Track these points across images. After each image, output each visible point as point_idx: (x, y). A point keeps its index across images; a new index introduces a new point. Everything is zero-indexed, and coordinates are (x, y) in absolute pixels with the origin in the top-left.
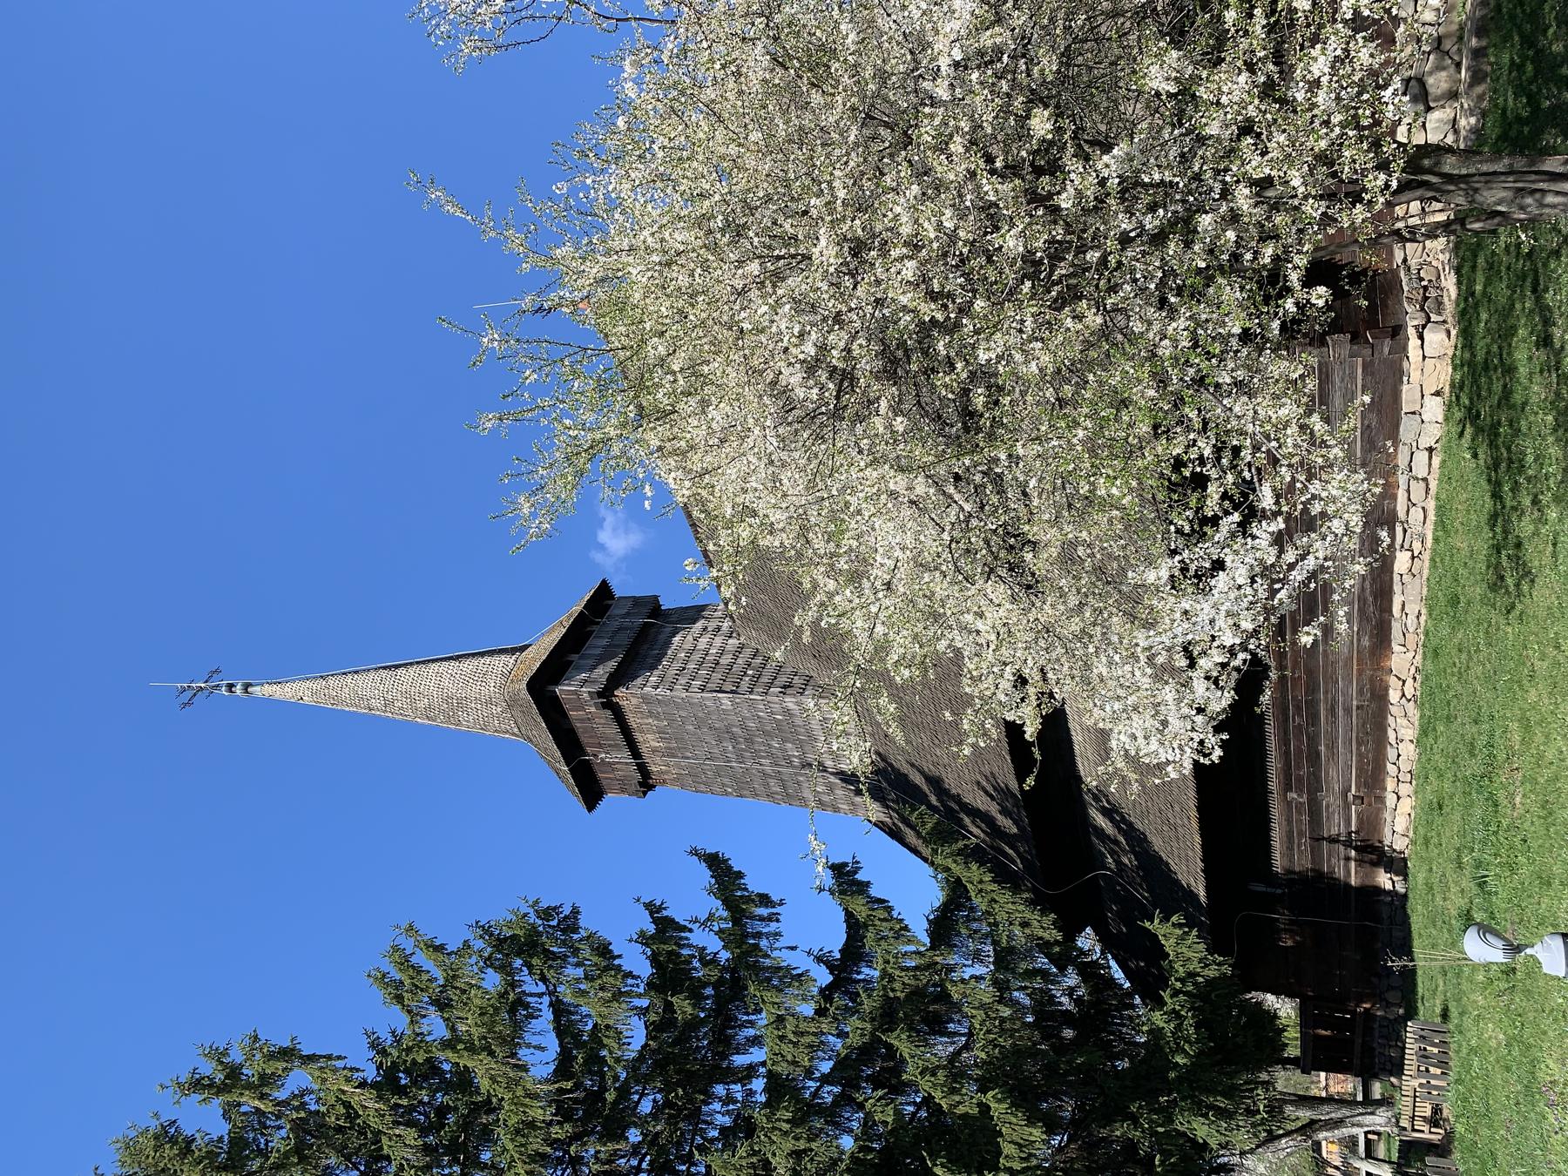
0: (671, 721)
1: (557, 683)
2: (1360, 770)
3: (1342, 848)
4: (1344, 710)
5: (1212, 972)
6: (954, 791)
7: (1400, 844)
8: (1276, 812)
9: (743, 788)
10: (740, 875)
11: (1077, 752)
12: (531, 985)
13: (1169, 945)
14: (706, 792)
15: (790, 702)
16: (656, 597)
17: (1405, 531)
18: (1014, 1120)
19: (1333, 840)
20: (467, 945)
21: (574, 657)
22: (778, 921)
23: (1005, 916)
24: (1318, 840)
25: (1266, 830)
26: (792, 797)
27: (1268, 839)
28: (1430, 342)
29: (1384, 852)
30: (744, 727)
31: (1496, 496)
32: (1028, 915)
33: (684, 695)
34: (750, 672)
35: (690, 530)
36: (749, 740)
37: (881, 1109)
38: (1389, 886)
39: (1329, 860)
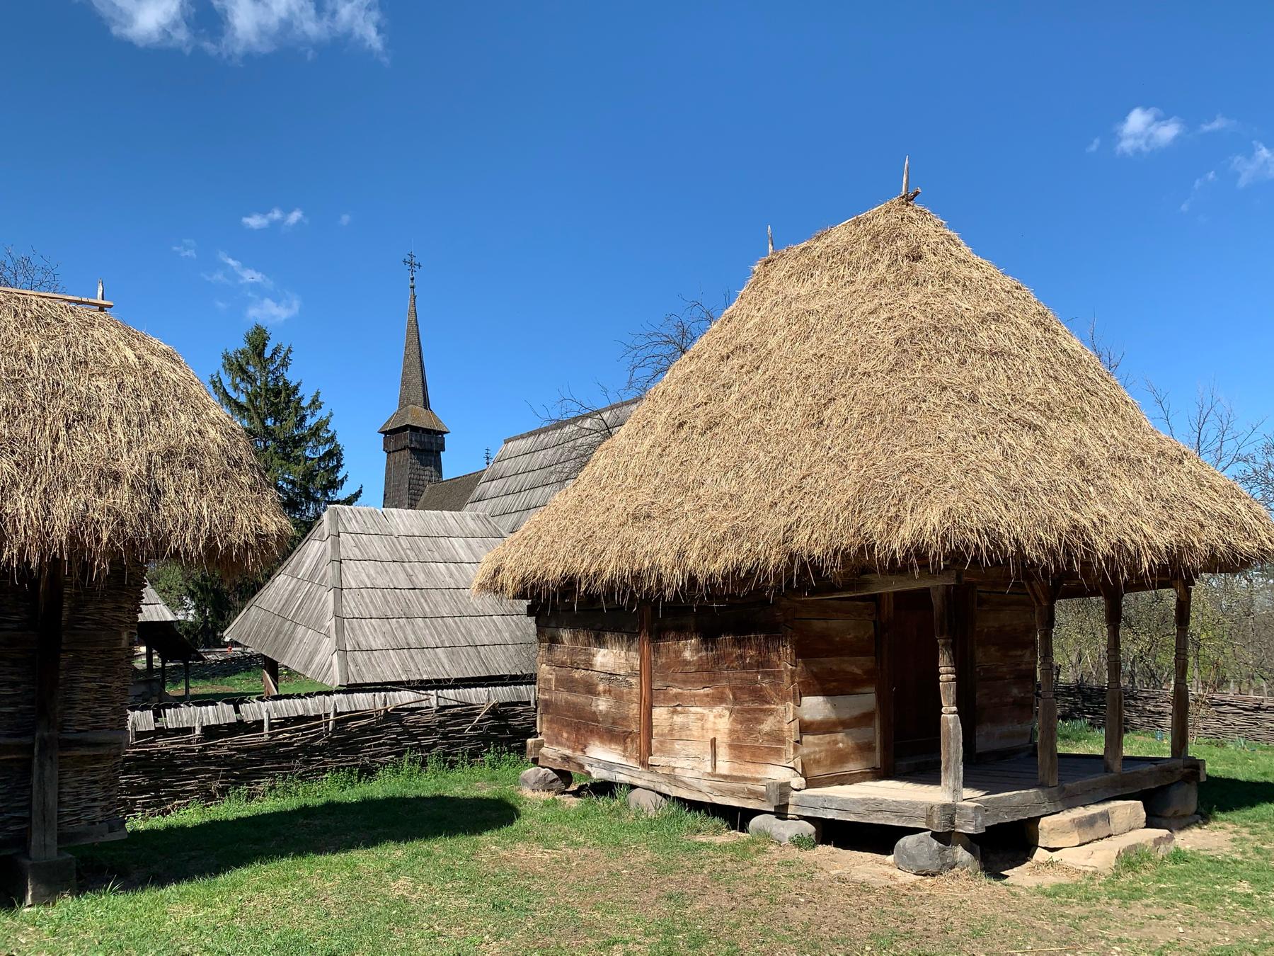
0: (402, 466)
9: (387, 484)
20: (329, 431)
21: (421, 431)
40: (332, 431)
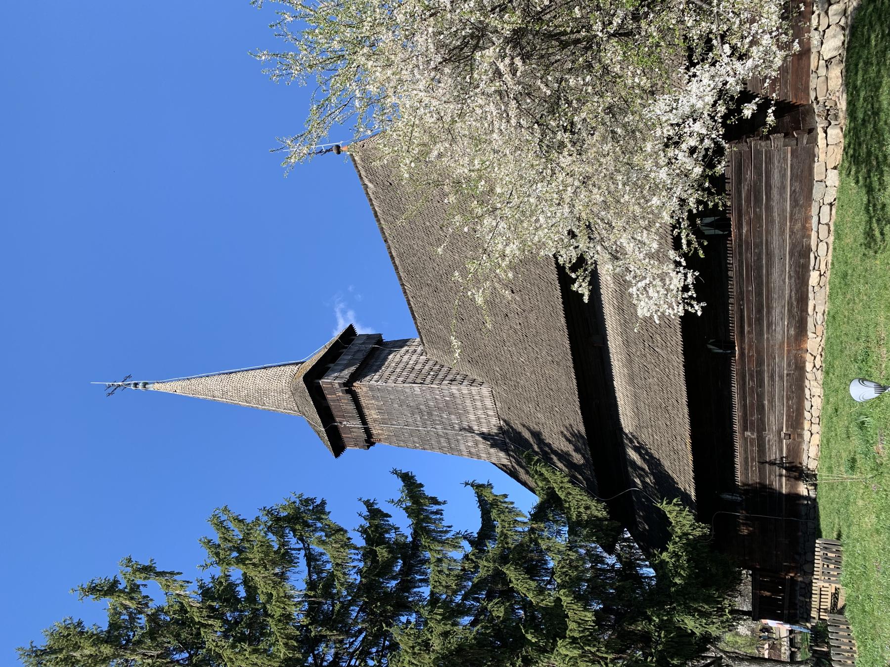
1: (320, 379)
2: (788, 416)
3: (777, 468)
4: (779, 377)
5: (697, 533)
6: (547, 441)
7: (812, 465)
8: (738, 445)
10: (421, 485)
11: (620, 412)
12: (293, 542)
13: (671, 517)
14: (404, 447)
15: (454, 389)
16: (380, 335)
17: (816, 258)
18: (575, 607)
19: (772, 463)
20: (257, 519)
21: (332, 365)
22: (441, 514)
23: (576, 503)
24: (763, 463)
25: (733, 457)
26: (453, 450)
27: (733, 463)
28: (831, 135)
29: (802, 471)
30: (427, 406)
31: (870, 190)
32: (589, 502)
33: (393, 385)
34: (432, 373)
35: (401, 287)
36: (430, 414)
37: (495, 609)
38: (805, 493)
39: (770, 477)
40: (260, 514)
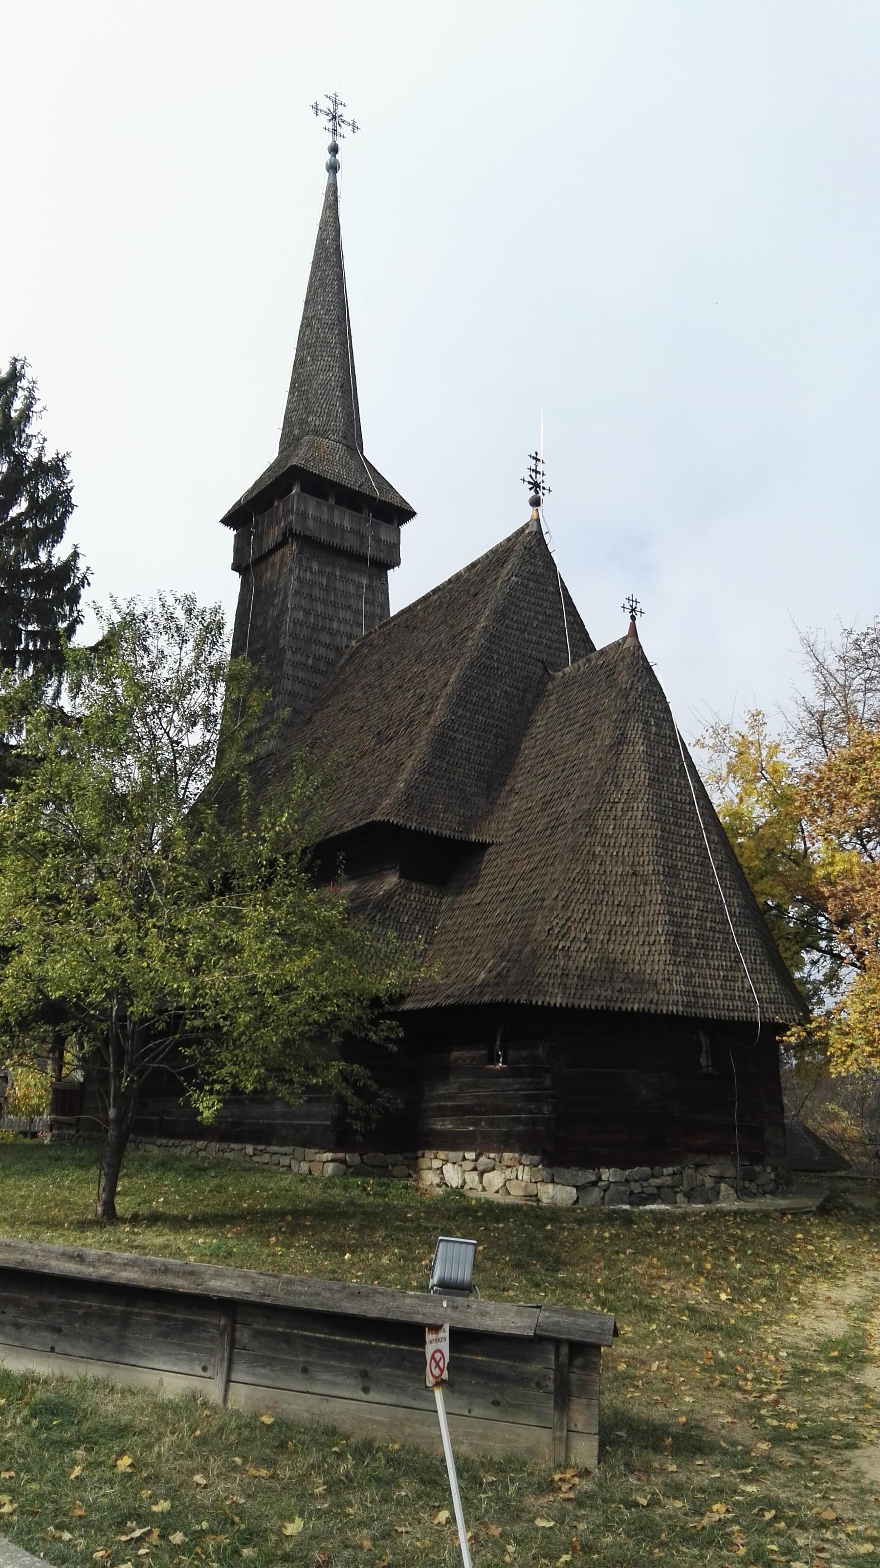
21: (332, 501)
